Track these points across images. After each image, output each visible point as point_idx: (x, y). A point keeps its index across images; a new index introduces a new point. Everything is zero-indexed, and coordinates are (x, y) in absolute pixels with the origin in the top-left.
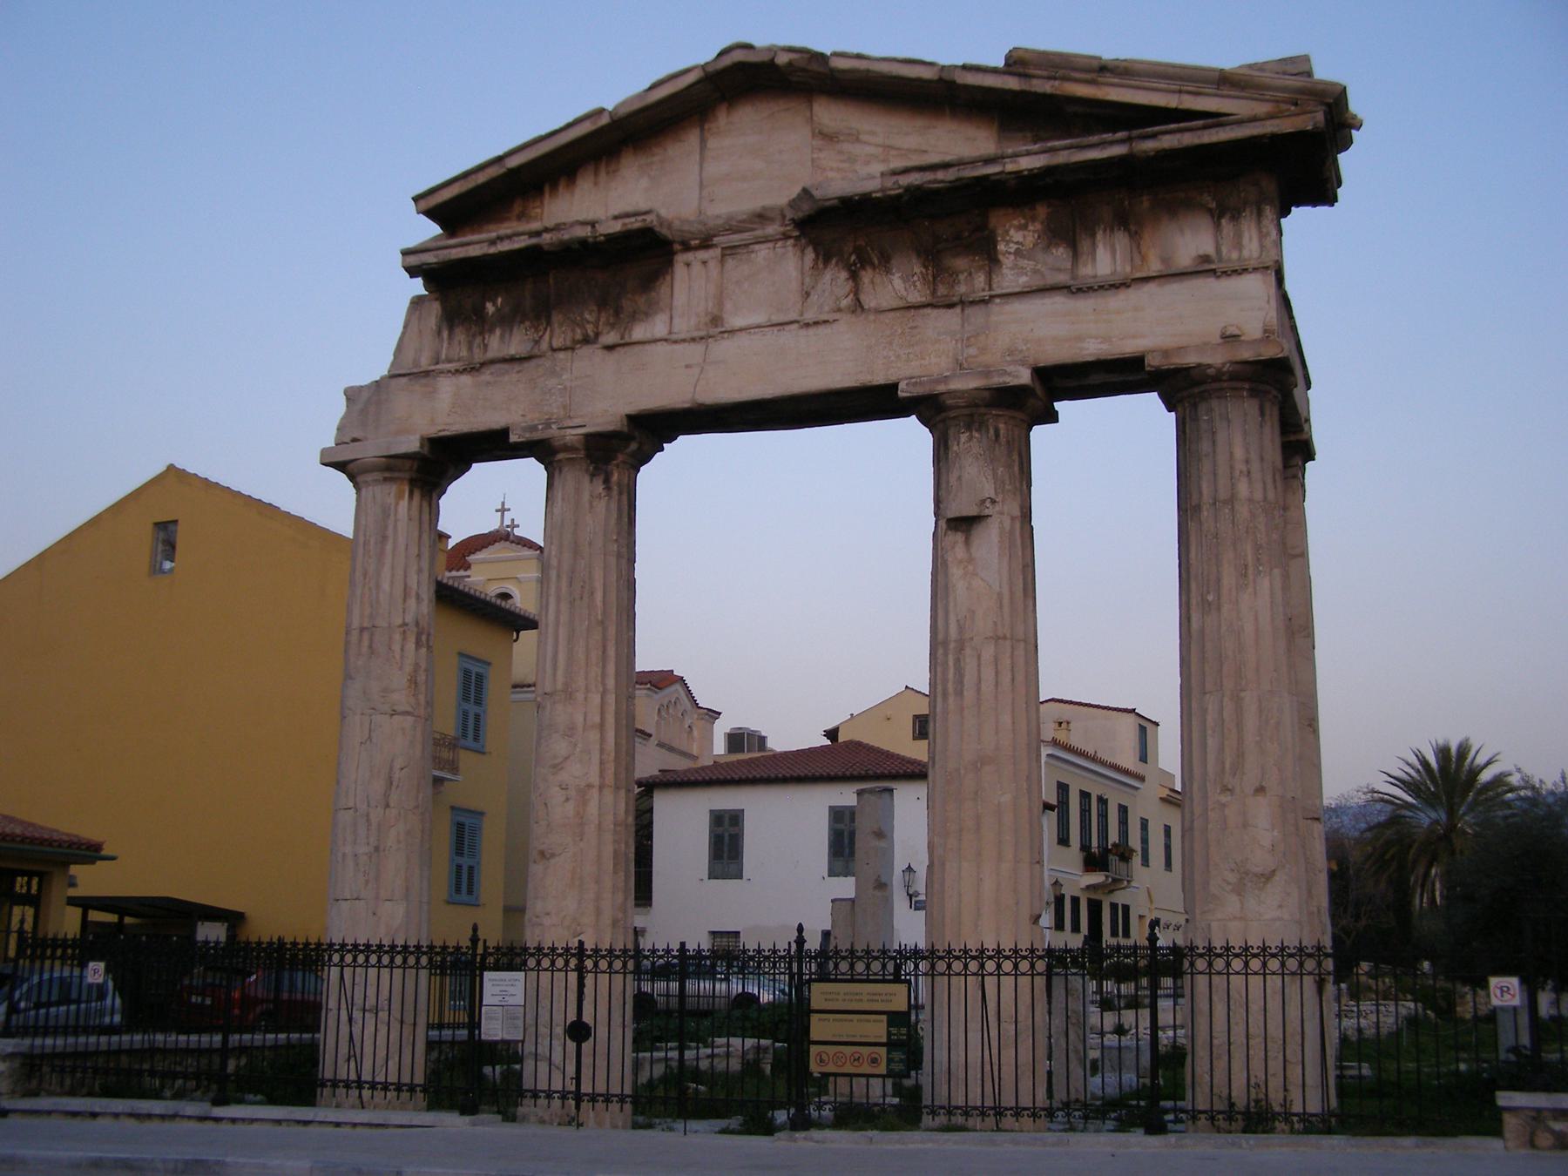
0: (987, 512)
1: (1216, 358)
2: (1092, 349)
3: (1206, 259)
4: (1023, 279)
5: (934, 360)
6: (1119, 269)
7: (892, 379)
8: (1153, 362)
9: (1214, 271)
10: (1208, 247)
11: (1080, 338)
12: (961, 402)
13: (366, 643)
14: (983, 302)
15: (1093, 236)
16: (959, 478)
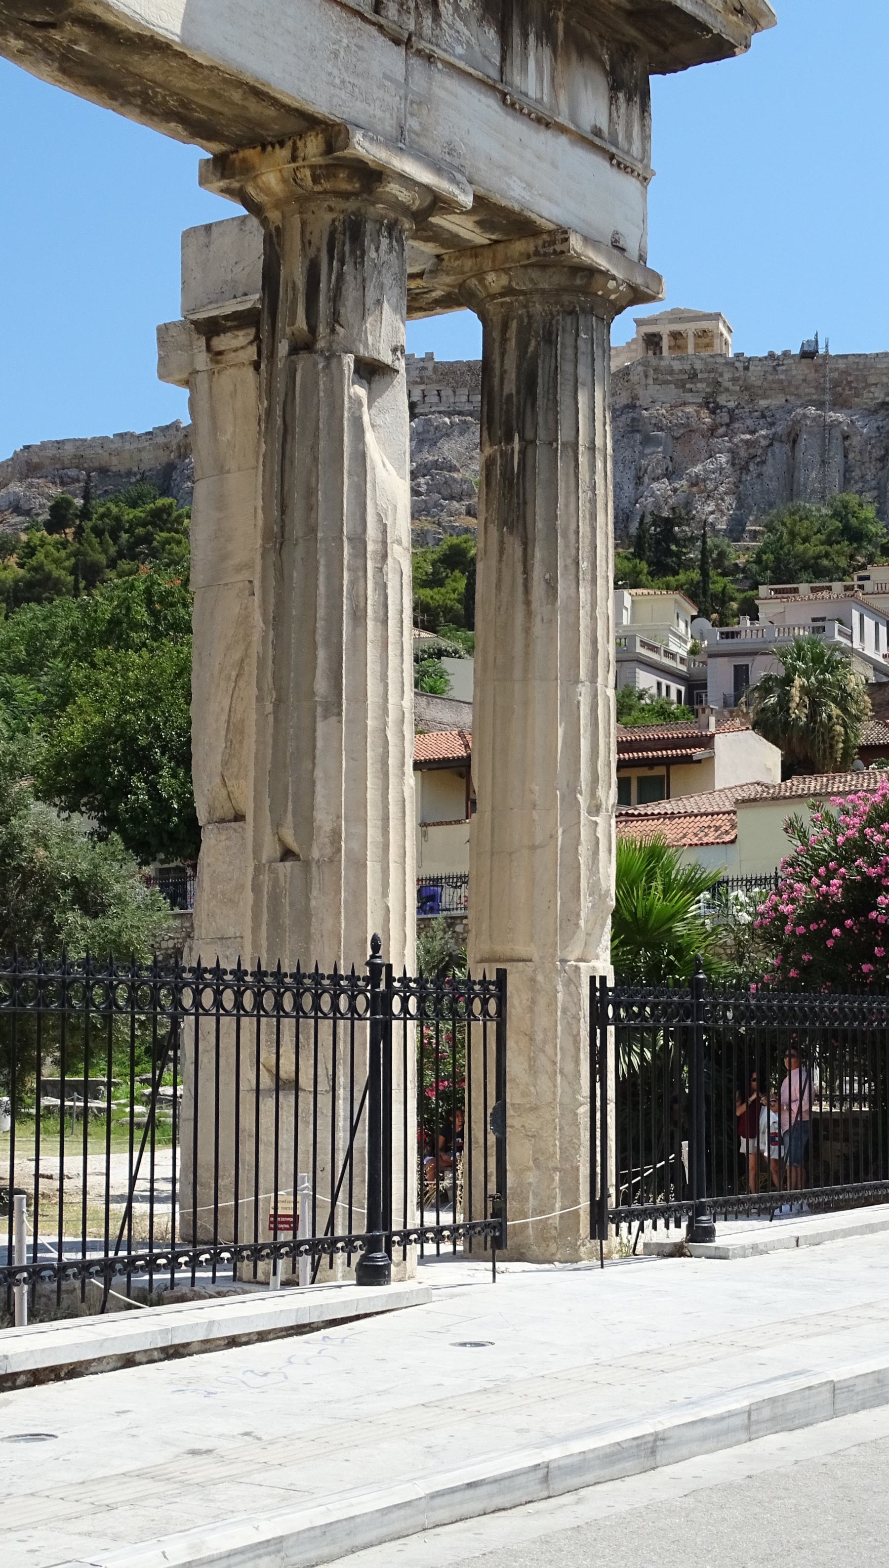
2: (514, 193)
3: (597, 132)
5: (379, 113)
6: (545, 99)
9: (612, 157)
10: (603, 123)
11: (507, 171)
12: (404, 195)
14: (430, 58)
15: (525, 36)
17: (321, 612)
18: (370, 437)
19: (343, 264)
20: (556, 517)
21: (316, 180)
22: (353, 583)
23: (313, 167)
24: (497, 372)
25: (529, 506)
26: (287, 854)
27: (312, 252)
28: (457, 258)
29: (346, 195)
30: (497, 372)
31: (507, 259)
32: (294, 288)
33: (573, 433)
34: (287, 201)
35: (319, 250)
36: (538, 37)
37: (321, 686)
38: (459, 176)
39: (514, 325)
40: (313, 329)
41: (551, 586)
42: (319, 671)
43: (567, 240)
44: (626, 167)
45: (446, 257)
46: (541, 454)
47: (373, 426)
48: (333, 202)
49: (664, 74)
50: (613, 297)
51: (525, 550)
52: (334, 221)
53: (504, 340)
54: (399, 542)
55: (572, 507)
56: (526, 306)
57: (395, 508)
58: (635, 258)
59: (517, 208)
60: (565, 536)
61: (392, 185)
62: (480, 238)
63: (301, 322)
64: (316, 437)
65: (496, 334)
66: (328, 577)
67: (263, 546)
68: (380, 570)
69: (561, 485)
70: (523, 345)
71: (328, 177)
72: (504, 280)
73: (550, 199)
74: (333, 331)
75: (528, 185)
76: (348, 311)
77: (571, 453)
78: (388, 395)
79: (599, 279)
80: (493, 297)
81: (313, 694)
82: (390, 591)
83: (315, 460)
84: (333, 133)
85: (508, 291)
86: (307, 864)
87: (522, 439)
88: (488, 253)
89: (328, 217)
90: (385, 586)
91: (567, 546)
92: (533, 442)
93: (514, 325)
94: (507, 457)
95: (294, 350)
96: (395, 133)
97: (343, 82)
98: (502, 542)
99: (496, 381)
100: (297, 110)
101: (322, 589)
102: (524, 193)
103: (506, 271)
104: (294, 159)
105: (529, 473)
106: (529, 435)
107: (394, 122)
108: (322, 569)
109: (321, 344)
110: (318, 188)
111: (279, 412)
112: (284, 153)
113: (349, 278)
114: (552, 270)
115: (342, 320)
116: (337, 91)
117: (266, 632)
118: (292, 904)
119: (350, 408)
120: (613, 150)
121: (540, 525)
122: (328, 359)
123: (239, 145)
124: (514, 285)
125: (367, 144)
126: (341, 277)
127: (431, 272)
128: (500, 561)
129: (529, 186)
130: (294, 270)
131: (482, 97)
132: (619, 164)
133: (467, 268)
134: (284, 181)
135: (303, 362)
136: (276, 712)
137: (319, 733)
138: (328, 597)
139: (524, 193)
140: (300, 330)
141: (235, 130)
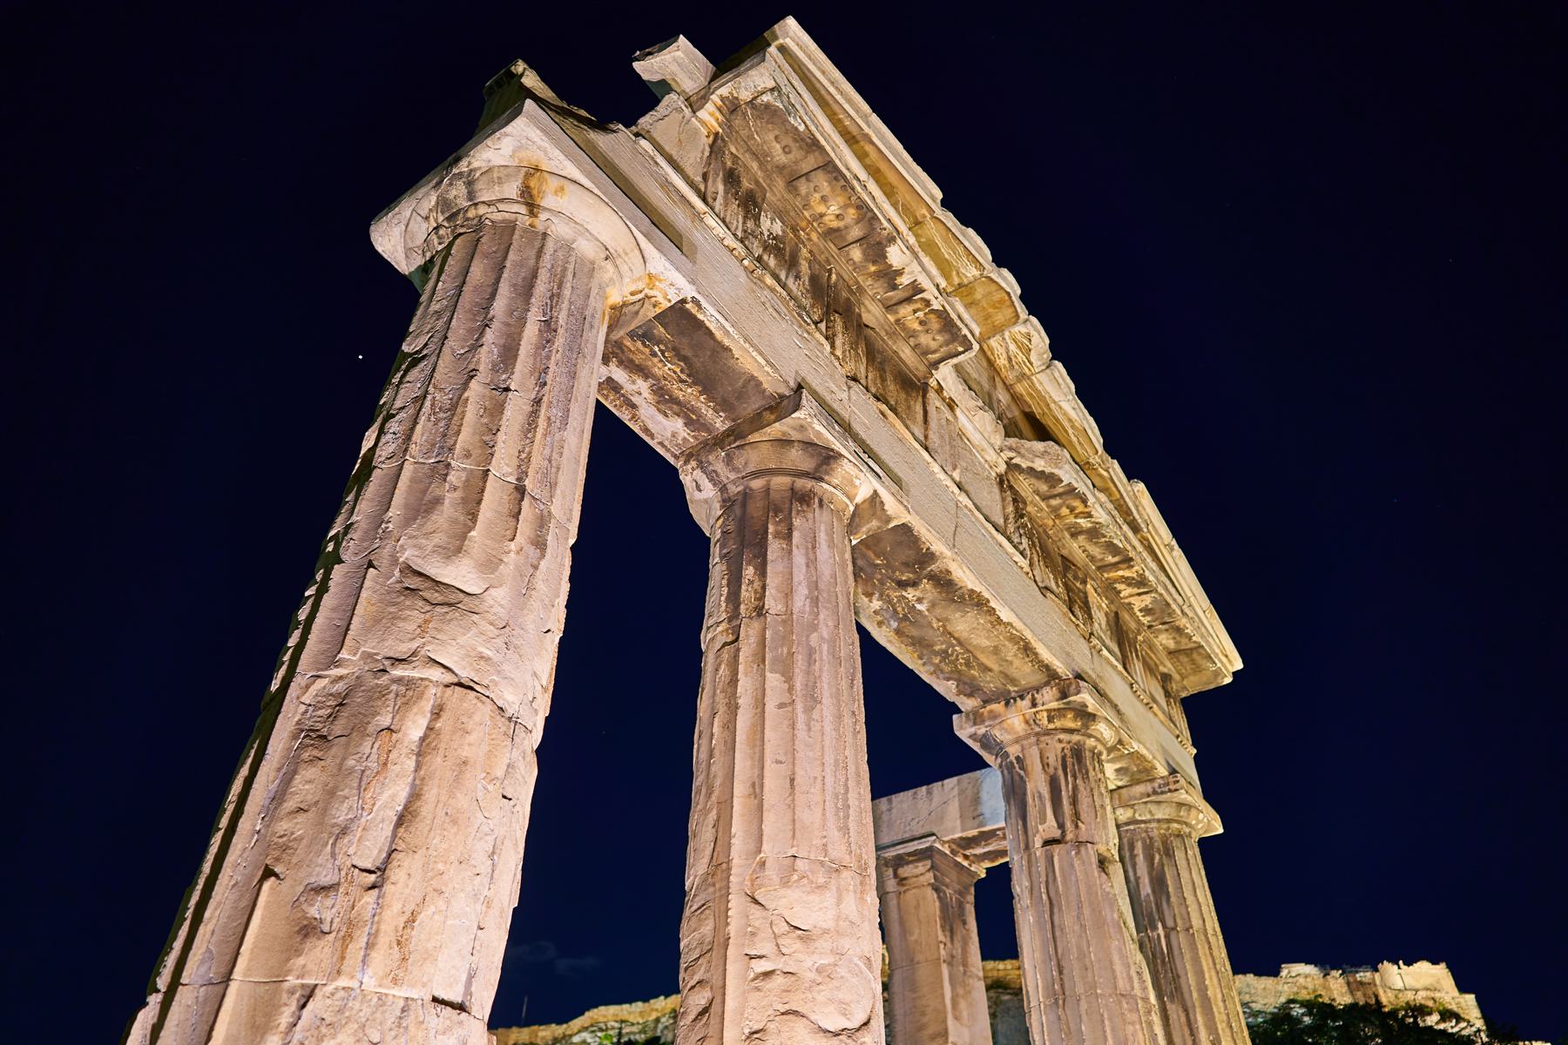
13: (525, 527)
20: (1206, 989)
21: (1050, 720)
27: (1051, 771)
29: (1071, 731)
32: (1040, 797)
34: (1027, 737)
39: (1139, 845)
46: (1182, 939)
48: (1062, 736)
53: (1133, 857)
64: (1080, 908)
70: (1150, 859)
74: (1077, 826)
92: (1174, 929)
93: (1139, 845)
104: (1034, 705)
105: (1176, 952)
106: (1170, 923)
109: (1069, 836)
110: (1051, 726)
113: (1081, 788)
121: (1195, 995)
123: (986, 702)
126: (1075, 788)
130: (1037, 784)
135: (1057, 849)
141: (990, 683)
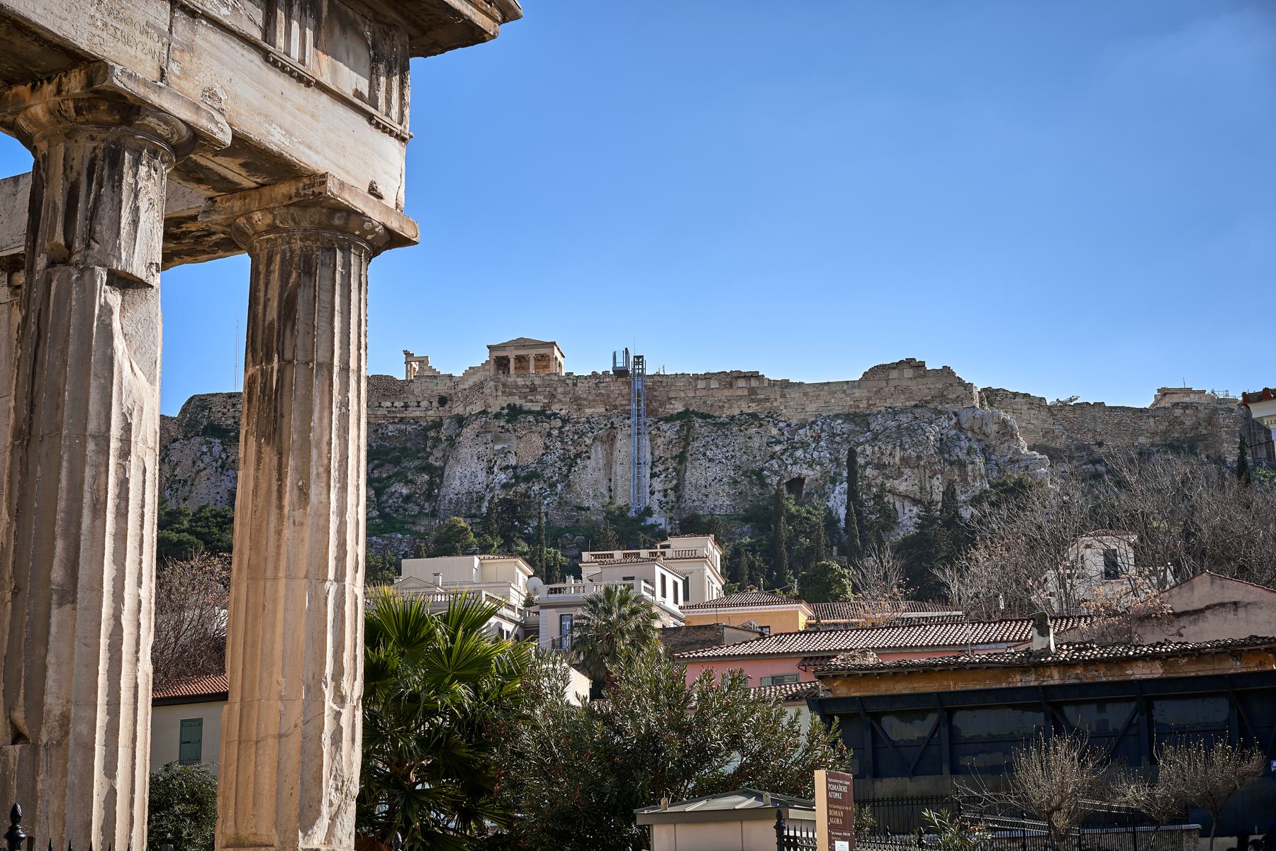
0: (151, 281)
1: (375, 213)
2: (275, 138)
3: (358, 94)
4: (224, 11)
7: (98, 51)
8: (332, 187)
11: (269, 119)
12: (162, 129)
16: (135, 222)
17: (62, 505)
18: (119, 343)
19: (101, 187)
21: (78, 111)
22: (95, 478)
23: (76, 100)
24: (262, 301)
25: (286, 420)
26: (18, 737)
27: (73, 176)
28: (228, 200)
30: (262, 301)
31: (272, 200)
32: (55, 208)
33: (328, 355)
35: (79, 174)
36: (303, 9)
37: (58, 574)
38: (217, 116)
40: (69, 245)
41: (303, 493)
42: (56, 562)
43: (324, 183)
44: (385, 127)
45: (218, 199)
46: (296, 375)
47: (125, 335)
48: (94, 130)
49: (425, 56)
50: (369, 237)
51: (280, 459)
52: (95, 149)
53: (269, 273)
54: (145, 441)
55: (326, 421)
56: (289, 243)
57: (142, 409)
58: (393, 206)
59: (275, 149)
60: (318, 447)
61: (150, 119)
62: (247, 182)
63: (59, 238)
64: (67, 342)
65: (262, 268)
66: (71, 472)
67: (13, 444)
68: (123, 468)
69: (317, 401)
70: (285, 277)
71: (89, 110)
72: (268, 219)
73: (310, 147)
74: (88, 246)
75: (288, 132)
76: (102, 229)
77: (326, 372)
78: (142, 309)
79: (354, 222)
80: (259, 234)
81: (49, 582)
82: (132, 486)
83: (65, 362)
84: (93, 66)
85: (272, 228)
86: (35, 747)
87: (281, 358)
88: (255, 194)
89: (91, 145)
90: (127, 481)
91: (320, 456)
92: (290, 362)
94: (266, 375)
95: (52, 263)
96: (156, 75)
97: (105, 24)
98: (259, 452)
99: (261, 308)
100: (58, 46)
101: (64, 482)
102: (283, 139)
103: (271, 211)
104: (59, 92)
106: (288, 355)
107: (156, 65)
108: (65, 464)
111: (33, 319)
112: (49, 89)
114: (312, 210)
115: (97, 236)
116: (99, 32)
117: (10, 524)
118: (19, 787)
119: (100, 316)
120: (372, 110)
122: (82, 271)
124: (278, 222)
125: (125, 79)
126: (98, 198)
127: (205, 212)
128: (257, 469)
129: (289, 134)
131: (245, 52)
132: (377, 125)
133: (236, 209)
134: (51, 112)
135: (59, 273)
136: (13, 600)
137: (54, 620)
138: (69, 492)
139: (283, 139)
140: (58, 245)
